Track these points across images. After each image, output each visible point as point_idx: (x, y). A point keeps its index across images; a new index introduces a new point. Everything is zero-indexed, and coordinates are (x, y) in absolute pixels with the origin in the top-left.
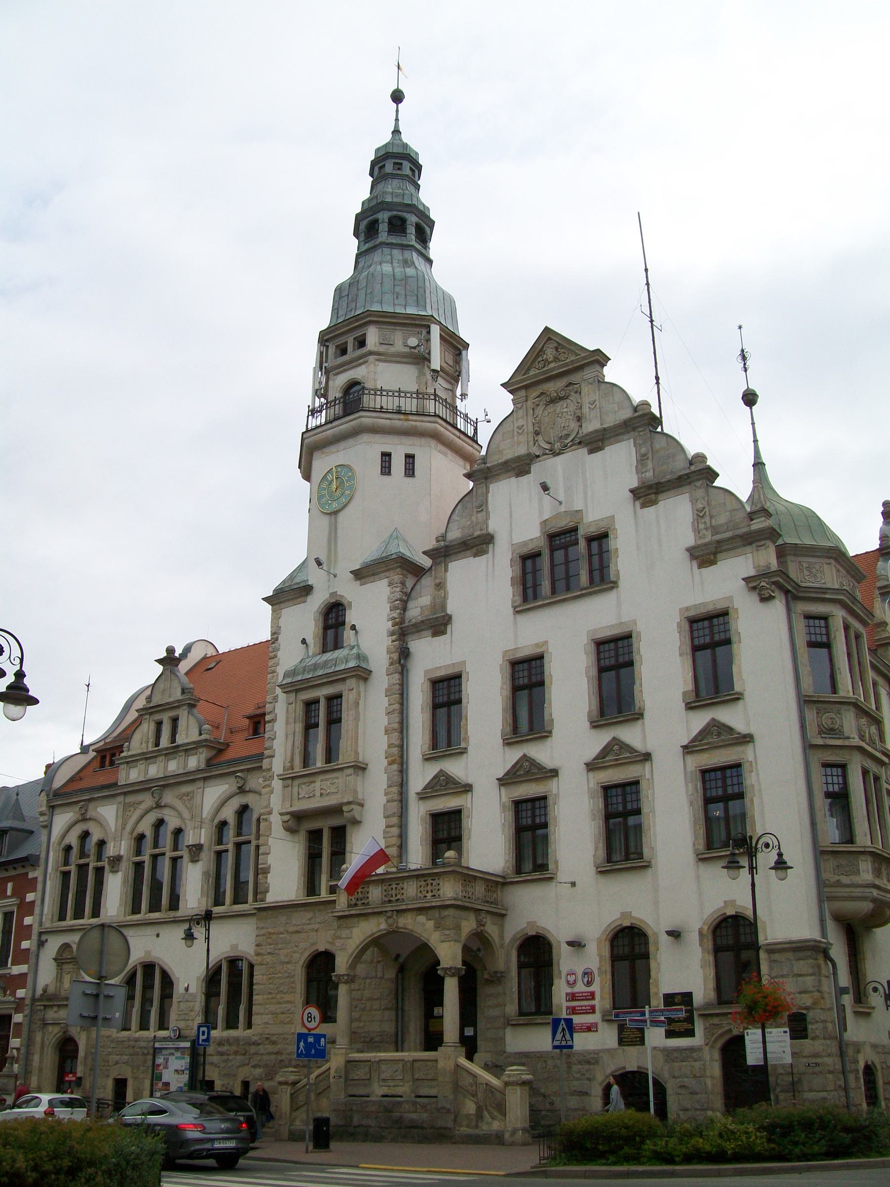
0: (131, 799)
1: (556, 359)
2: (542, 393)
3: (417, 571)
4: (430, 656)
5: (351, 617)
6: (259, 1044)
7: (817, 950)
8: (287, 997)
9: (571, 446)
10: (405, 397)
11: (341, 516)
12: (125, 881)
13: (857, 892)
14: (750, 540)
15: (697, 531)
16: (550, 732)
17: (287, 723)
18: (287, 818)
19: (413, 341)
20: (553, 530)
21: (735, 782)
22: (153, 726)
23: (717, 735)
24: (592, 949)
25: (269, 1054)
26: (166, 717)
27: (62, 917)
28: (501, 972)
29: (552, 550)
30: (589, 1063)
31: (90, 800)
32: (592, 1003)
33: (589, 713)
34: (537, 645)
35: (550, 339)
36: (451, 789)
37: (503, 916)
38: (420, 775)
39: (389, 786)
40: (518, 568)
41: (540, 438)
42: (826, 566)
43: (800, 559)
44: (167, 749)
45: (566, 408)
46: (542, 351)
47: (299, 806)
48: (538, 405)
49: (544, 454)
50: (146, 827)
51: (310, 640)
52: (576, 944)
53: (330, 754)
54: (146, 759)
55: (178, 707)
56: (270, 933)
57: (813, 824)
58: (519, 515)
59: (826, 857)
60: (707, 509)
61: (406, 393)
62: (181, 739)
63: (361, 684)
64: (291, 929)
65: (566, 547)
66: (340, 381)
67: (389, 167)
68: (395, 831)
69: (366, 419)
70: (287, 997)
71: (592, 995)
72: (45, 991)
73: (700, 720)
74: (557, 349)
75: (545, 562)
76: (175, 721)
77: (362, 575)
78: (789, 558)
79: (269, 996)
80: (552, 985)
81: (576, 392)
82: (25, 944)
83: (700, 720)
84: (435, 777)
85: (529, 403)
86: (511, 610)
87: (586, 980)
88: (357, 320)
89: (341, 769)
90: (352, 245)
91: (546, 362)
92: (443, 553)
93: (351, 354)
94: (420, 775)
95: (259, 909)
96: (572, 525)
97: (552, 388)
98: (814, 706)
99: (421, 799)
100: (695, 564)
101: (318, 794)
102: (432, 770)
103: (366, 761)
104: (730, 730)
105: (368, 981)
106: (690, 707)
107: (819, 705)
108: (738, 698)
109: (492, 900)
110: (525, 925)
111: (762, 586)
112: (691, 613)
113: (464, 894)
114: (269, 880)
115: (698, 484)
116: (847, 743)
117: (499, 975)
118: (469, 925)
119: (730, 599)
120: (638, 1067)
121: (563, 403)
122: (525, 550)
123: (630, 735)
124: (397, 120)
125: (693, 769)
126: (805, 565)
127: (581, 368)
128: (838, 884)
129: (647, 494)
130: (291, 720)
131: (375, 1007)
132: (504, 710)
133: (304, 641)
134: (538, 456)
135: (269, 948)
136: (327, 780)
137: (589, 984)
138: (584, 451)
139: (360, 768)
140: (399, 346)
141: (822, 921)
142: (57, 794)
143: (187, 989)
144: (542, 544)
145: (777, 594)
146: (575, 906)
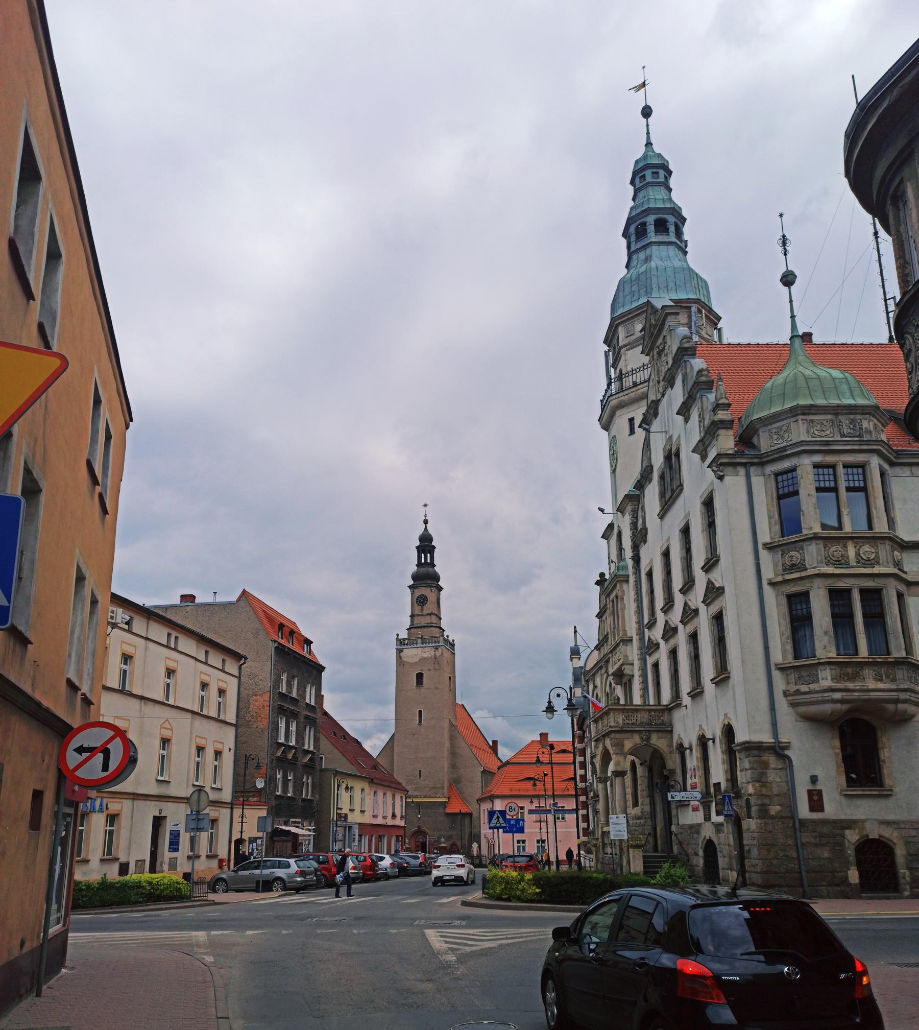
42: (793, 425)
43: (769, 427)
59: (789, 672)
67: (649, 178)
98: (779, 549)
124: (648, 133)
126: (774, 431)
128: (798, 692)
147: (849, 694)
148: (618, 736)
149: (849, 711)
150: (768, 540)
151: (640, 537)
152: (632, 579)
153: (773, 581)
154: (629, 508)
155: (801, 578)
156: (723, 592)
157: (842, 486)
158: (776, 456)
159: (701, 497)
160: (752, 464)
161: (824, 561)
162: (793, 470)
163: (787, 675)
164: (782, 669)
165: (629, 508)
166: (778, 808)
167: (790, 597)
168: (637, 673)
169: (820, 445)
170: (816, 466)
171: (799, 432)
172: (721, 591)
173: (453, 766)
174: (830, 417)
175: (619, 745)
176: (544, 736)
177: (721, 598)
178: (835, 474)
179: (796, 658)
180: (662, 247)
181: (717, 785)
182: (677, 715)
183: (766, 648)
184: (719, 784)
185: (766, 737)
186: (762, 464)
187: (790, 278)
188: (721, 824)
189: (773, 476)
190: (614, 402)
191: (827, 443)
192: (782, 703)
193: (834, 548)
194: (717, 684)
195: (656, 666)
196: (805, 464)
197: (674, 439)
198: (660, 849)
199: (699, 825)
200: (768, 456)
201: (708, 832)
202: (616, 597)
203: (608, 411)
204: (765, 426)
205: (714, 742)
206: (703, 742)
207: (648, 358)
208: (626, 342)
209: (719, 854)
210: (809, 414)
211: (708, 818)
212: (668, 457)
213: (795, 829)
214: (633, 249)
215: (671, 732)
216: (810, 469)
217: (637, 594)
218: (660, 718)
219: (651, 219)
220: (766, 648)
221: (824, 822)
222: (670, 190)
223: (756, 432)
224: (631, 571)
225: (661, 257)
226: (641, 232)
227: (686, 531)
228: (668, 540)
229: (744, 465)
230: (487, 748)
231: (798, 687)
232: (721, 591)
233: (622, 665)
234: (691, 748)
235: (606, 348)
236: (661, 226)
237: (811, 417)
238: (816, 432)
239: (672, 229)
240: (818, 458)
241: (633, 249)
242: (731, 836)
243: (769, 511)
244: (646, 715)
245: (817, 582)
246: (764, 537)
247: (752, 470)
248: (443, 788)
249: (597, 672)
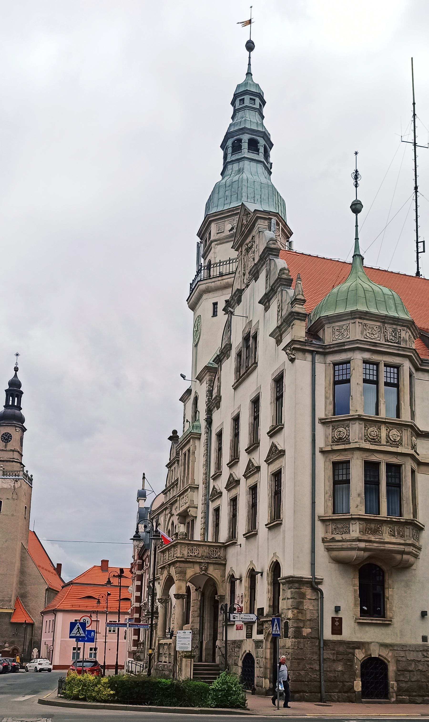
13: (346, 545)
43: (333, 325)
78: (326, 326)
126: (337, 328)
128: (333, 540)
147: (371, 544)
148: (182, 565)
149: (369, 557)
150: (323, 416)
151: (214, 403)
152: (203, 437)
153: (323, 450)
154: (207, 377)
155: (345, 450)
156: (284, 455)
157: (382, 380)
158: (336, 349)
159: (273, 374)
160: (318, 353)
161: (364, 438)
162: (348, 362)
163: (326, 525)
164: (323, 521)
165: (207, 377)
166: (309, 630)
167: (335, 464)
168: (200, 515)
169: (370, 345)
170: (365, 362)
171: (355, 332)
172: (282, 453)
173: (21, 583)
174: (379, 324)
175: (183, 573)
176: (105, 562)
177: (281, 459)
178: (377, 370)
179: (334, 513)
180: (253, 164)
181: (261, 610)
182: (232, 552)
183: (313, 503)
184: (263, 609)
185: (306, 574)
186: (325, 354)
187: (358, 206)
188: (261, 641)
189: (332, 365)
190: (202, 287)
191: (375, 344)
192: (320, 547)
193: (371, 429)
194: (270, 528)
195: (217, 510)
196: (358, 358)
197: (254, 324)
198: (203, 659)
199: (241, 641)
200: (330, 348)
201: (248, 647)
202: (189, 451)
203: (196, 294)
204: (330, 323)
205: (262, 575)
206: (252, 575)
207: (237, 253)
208: (217, 237)
209: (256, 665)
210: (364, 319)
211: (249, 636)
212: (246, 339)
213: (320, 647)
214: (228, 160)
215: (225, 565)
216: (360, 363)
217: (207, 450)
218: (218, 553)
219: (246, 138)
220: (313, 503)
221: (341, 643)
222: (263, 117)
223: (323, 327)
224: (203, 430)
225: (251, 171)
226: (237, 147)
227: (256, 402)
228: (239, 407)
229: (311, 352)
230: (52, 570)
231: (333, 536)
232: (282, 453)
233: (188, 507)
234: (240, 579)
235: (199, 240)
236: (253, 145)
237: (365, 322)
238: (368, 334)
239: (262, 150)
240: (367, 356)
241: (228, 160)
242: (268, 651)
243: (326, 392)
244: (207, 550)
245: (357, 454)
246: (321, 413)
247: (317, 357)
248: (10, 601)
249: (162, 512)
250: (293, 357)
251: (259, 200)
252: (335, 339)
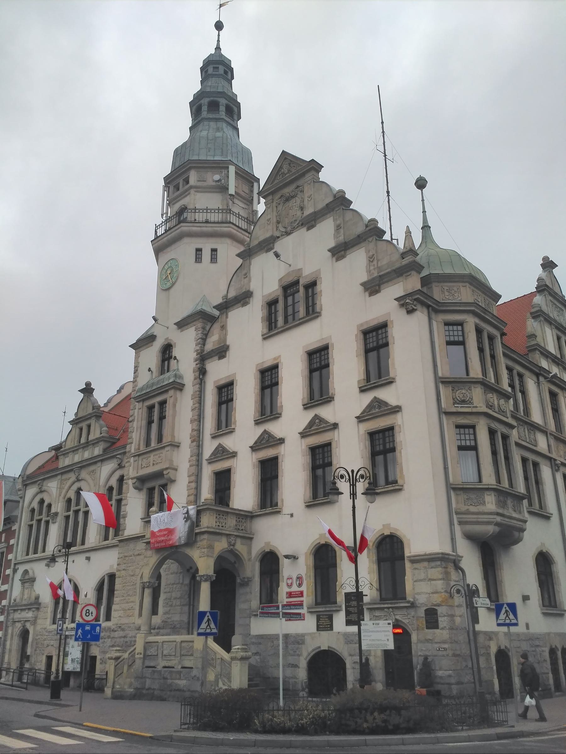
0: (65, 477)
1: (289, 171)
2: (282, 196)
3: (212, 319)
4: (217, 371)
5: (176, 352)
6: (116, 631)
7: (449, 562)
8: (132, 599)
9: (297, 227)
10: (211, 212)
11: (172, 290)
12: (59, 527)
14: (400, 272)
15: (369, 271)
16: (281, 414)
17: (138, 421)
18: (135, 480)
19: (217, 177)
20: (286, 284)
21: (391, 440)
22: (78, 431)
23: (378, 409)
24: (302, 560)
25: (121, 637)
26: (84, 425)
27: (27, 554)
28: (248, 578)
29: (286, 297)
30: (298, 643)
31: (44, 479)
32: (301, 599)
33: (303, 399)
34: (275, 359)
35: (286, 158)
36: (225, 455)
37: (251, 539)
38: (209, 447)
39: (191, 456)
40: (266, 312)
41: (280, 225)
44: (83, 444)
45: (295, 203)
46: (281, 167)
47: (142, 472)
48: (279, 204)
49: (282, 235)
50: (72, 494)
51: (154, 369)
52: (293, 558)
53: (160, 439)
54: (73, 451)
55: (90, 418)
56: (125, 557)
57: (446, 468)
58: (267, 277)
59: (459, 492)
60: (375, 256)
61: (211, 210)
62: (91, 437)
63: (178, 393)
64: (136, 553)
65: (293, 295)
66: (177, 207)
68: (193, 485)
69: (184, 228)
70: (132, 599)
71: (301, 594)
72: (15, 600)
73: (368, 398)
74: (290, 164)
75: (280, 306)
76: (89, 426)
77: (182, 325)
79: (123, 598)
80: (278, 586)
81: (301, 192)
82: (8, 572)
83: (368, 398)
84: (216, 448)
85: (274, 203)
86: (260, 338)
87: (298, 583)
88: (184, 167)
89: (164, 447)
90: (189, 122)
91: (283, 174)
92: (225, 306)
93: (181, 189)
94: (209, 447)
95: (120, 541)
96: (296, 279)
97: (287, 191)
99: (210, 463)
100: (367, 294)
101: (151, 464)
102: (215, 443)
103: (180, 442)
104: (386, 404)
105: (175, 586)
106: (363, 390)
107: (454, 385)
108: (391, 382)
109: (243, 528)
110: (262, 545)
111: (408, 303)
112: (365, 327)
113: (218, 524)
114: (126, 522)
115: (370, 239)
116: (474, 410)
117: (246, 580)
118: (221, 545)
119: (389, 314)
120: (329, 647)
121: (293, 200)
122: (270, 298)
123: (326, 413)
125: (364, 432)
127: (303, 175)
128: (468, 513)
129: (339, 251)
130: (140, 419)
131: (177, 604)
132: (256, 402)
133: (150, 370)
134: (278, 237)
135: (123, 567)
136: (156, 455)
137: (300, 585)
138: (304, 229)
139: (176, 446)
140: (210, 182)
141: (453, 540)
142: (29, 477)
143: (86, 596)
144: (280, 293)
145: (419, 307)
146: (294, 531)
185: (447, 549)
250: (415, 308)
251: (241, 162)
252: (444, 298)
